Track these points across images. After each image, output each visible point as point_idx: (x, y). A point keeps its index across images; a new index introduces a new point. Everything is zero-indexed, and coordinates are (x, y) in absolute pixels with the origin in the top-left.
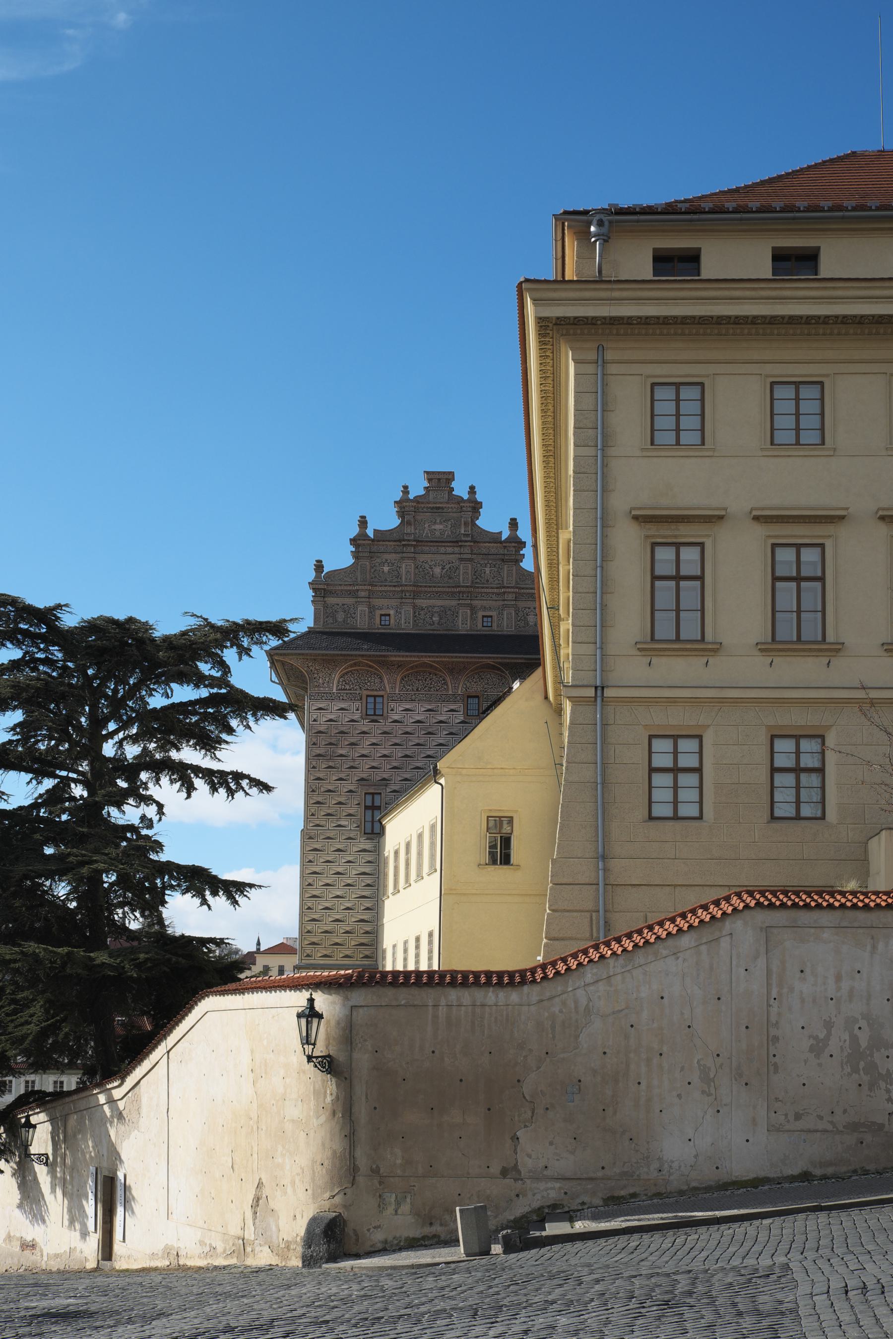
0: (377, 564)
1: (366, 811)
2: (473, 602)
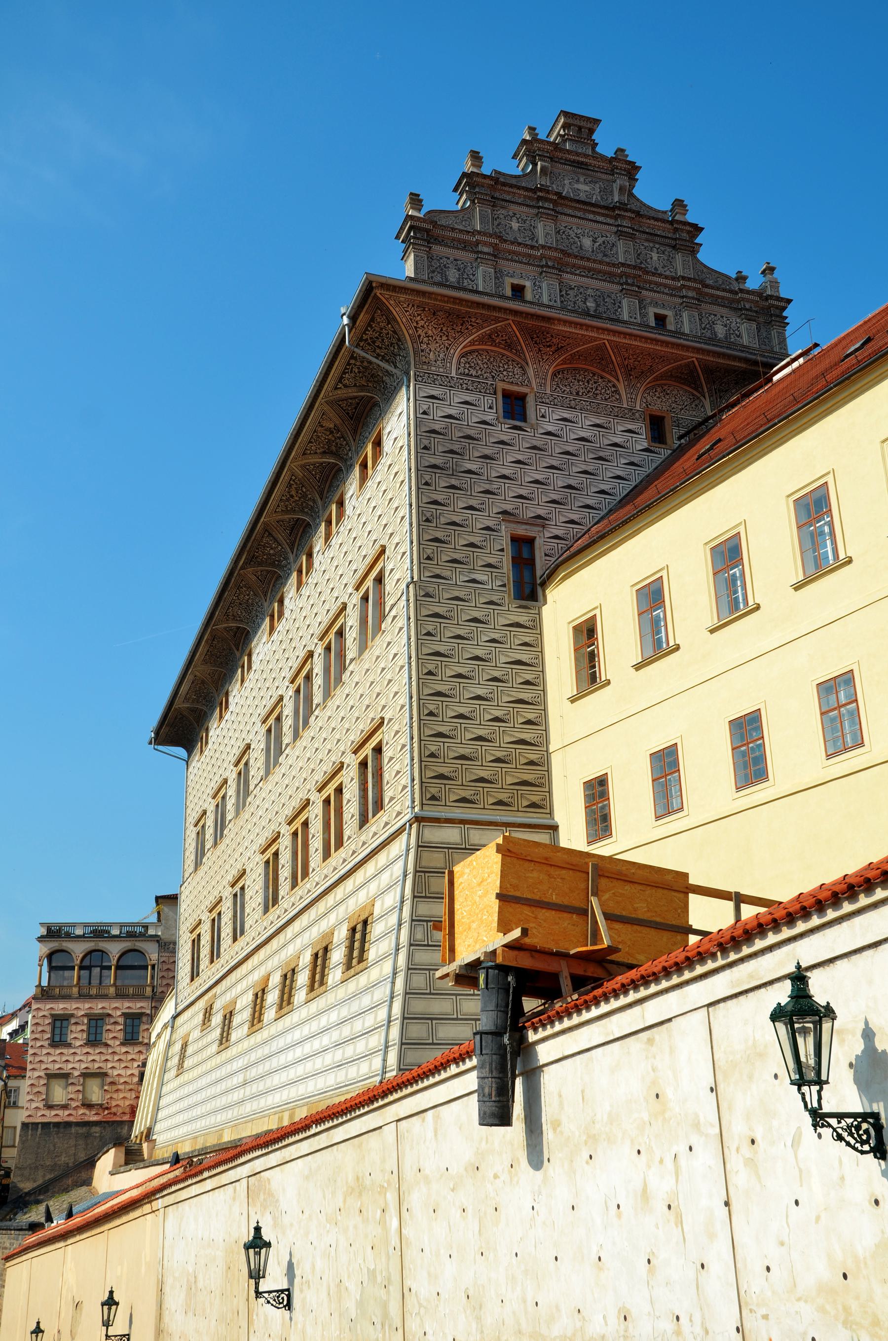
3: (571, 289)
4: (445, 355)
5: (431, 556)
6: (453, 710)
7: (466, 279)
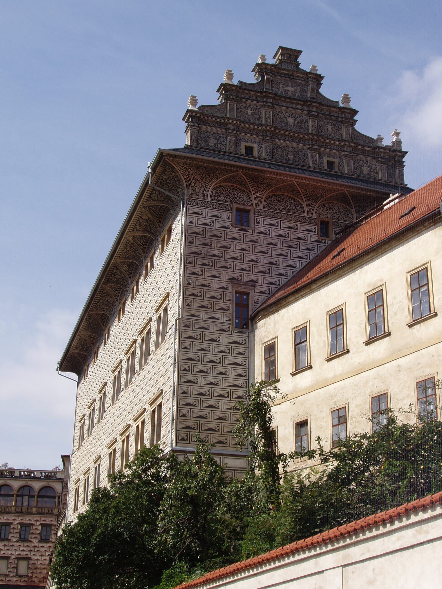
3: (280, 148)
5: (190, 304)
6: (197, 390)
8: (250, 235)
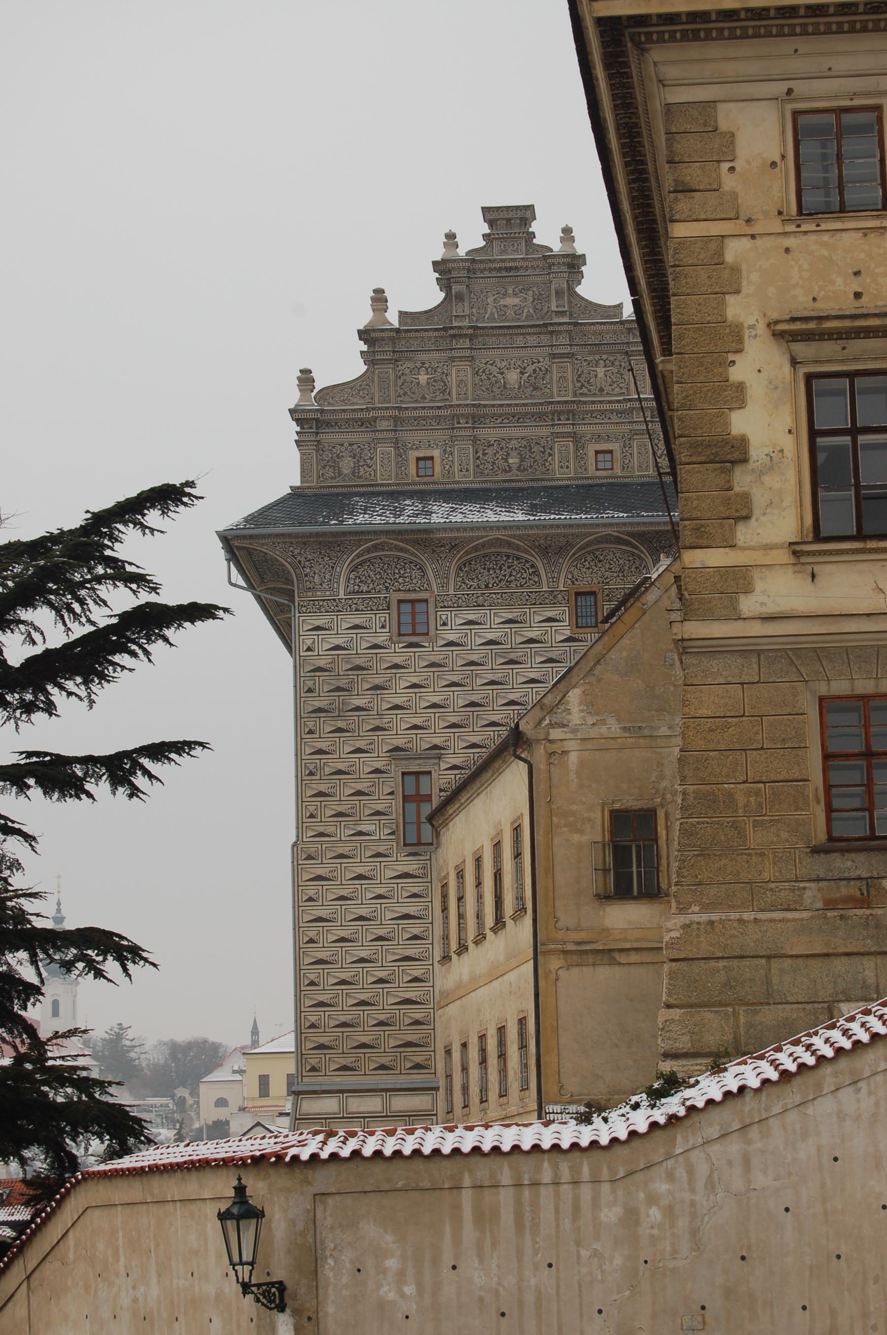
0: (407, 371)
1: (406, 805)
2: (578, 429)
4: (331, 575)
7: (362, 466)
8: (431, 652)
